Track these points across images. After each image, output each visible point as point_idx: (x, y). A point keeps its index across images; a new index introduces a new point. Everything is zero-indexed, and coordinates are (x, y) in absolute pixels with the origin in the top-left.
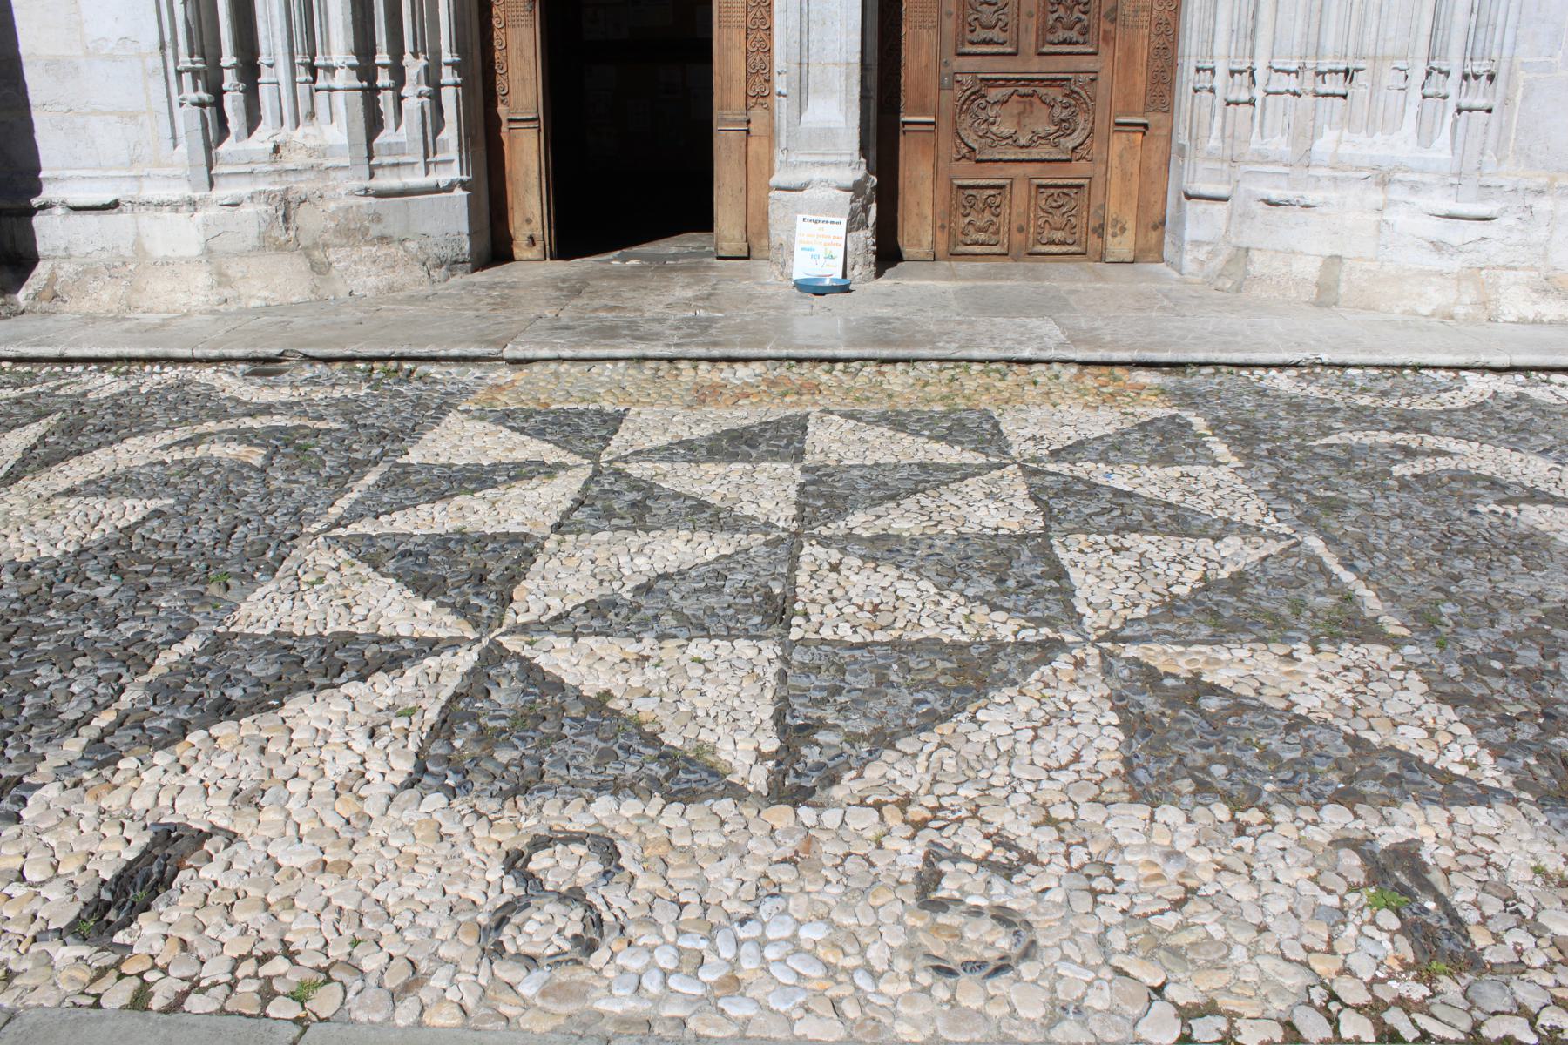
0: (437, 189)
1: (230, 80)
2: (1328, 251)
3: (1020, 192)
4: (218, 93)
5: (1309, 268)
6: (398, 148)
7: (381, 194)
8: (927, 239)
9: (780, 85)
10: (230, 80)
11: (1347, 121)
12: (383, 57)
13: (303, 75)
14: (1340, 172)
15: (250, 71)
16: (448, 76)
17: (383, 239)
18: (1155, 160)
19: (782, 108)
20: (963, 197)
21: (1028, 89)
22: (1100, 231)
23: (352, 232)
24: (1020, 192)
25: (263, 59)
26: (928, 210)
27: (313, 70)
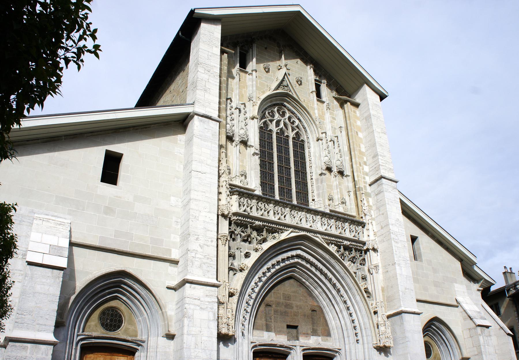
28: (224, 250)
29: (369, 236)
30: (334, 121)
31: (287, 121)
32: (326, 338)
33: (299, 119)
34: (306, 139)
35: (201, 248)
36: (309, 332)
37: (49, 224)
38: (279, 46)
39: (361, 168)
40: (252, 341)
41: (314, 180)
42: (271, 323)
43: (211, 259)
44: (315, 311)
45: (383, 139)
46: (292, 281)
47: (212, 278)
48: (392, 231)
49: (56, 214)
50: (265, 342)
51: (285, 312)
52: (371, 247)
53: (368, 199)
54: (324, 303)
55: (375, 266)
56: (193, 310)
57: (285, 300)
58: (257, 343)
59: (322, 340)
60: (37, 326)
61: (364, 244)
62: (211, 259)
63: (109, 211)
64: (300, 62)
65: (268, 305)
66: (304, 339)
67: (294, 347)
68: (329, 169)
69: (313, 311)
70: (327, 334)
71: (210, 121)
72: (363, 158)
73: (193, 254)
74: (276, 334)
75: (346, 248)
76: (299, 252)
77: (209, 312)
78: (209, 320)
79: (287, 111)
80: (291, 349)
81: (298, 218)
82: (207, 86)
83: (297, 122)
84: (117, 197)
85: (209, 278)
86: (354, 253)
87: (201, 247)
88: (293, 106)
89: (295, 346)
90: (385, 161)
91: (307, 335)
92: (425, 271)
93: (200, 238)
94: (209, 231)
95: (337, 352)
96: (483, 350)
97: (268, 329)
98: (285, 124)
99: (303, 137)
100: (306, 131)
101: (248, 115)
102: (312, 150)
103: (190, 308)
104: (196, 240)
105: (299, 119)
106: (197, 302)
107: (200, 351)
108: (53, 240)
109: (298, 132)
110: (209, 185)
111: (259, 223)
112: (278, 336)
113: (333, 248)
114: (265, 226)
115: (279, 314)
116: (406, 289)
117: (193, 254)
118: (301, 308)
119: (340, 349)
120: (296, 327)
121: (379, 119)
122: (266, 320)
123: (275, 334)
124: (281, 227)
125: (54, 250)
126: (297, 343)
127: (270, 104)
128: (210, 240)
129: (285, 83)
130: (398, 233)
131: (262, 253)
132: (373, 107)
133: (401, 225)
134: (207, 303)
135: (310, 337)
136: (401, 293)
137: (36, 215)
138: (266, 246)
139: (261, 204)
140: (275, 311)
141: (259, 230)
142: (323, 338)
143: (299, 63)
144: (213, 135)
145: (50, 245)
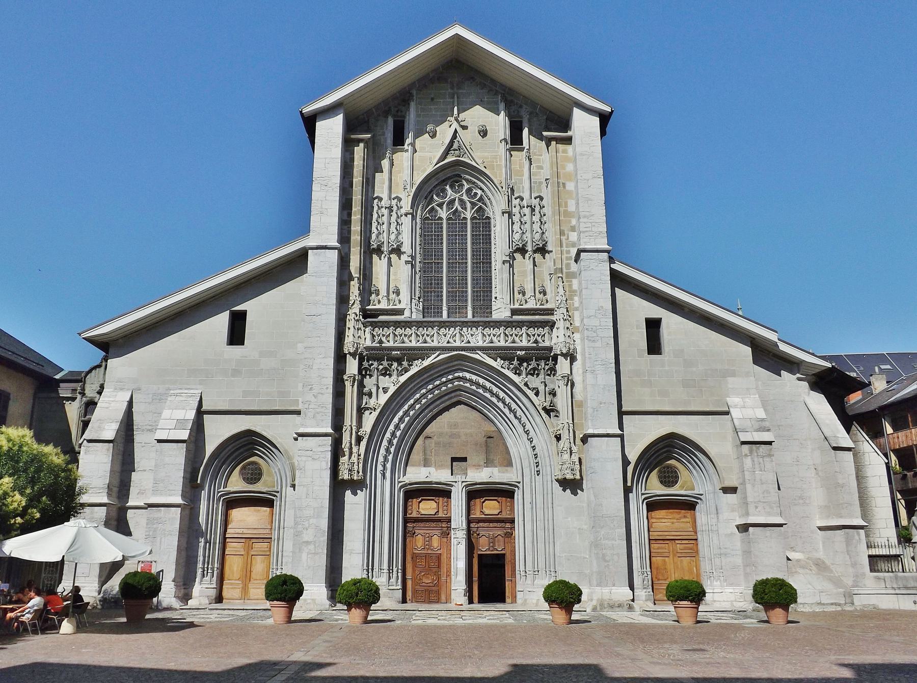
0: (398, 589)
1: (370, 570)
2: (537, 598)
4: (368, 573)
5: (535, 601)
6: (392, 582)
9: (452, 573)
10: (370, 570)
12: (391, 568)
13: (380, 570)
15: (372, 569)
16: (400, 571)
18: (513, 586)
19: (453, 577)
25: (374, 568)
27: (381, 569)
29: (558, 337)
30: (540, 172)
31: (465, 197)
33: (481, 189)
34: (491, 215)
35: (315, 398)
36: (482, 463)
38: (452, 88)
39: (563, 238)
41: (497, 270)
42: (431, 457)
43: (325, 407)
44: (492, 437)
45: (593, 188)
47: (327, 427)
48: (588, 328)
49: (188, 387)
50: (411, 480)
51: (449, 443)
52: (559, 353)
53: (571, 281)
55: (562, 377)
56: (305, 461)
58: (407, 482)
61: (550, 349)
62: (325, 407)
63: (236, 372)
64: (487, 98)
65: (427, 437)
66: (474, 472)
68: (522, 250)
69: (490, 437)
70: (508, 463)
72: (570, 222)
73: (306, 406)
74: (436, 470)
75: (521, 360)
77: (322, 461)
78: (321, 469)
79: (465, 183)
80: (452, 486)
82: (323, 207)
83: (479, 192)
87: (315, 396)
89: (456, 482)
91: (478, 466)
92: (667, 368)
93: (314, 388)
94: (324, 377)
96: (747, 477)
98: (462, 202)
99: (489, 212)
100: (491, 204)
101: (403, 211)
102: (498, 228)
104: (310, 390)
105: (481, 189)
108: (180, 414)
110: (325, 328)
111: (396, 352)
112: (439, 471)
113: (497, 364)
114: (405, 354)
115: (442, 445)
116: (601, 404)
117: (306, 406)
118: (472, 436)
119: (519, 483)
120: (464, 459)
122: (425, 454)
123: (436, 469)
125: (180, 424)
126: (459, 478)
129: (455, 146)
130: (598, 328)
131: (398, 386)
134: (320, 453)
136: (590, 411)
137: (172, 392)
138: (403, 379)
140: (435, 444)
141: (399, 360)
142: (500, 468)
143: (486, 100)
144: (330, 267)
145: (177, 420)
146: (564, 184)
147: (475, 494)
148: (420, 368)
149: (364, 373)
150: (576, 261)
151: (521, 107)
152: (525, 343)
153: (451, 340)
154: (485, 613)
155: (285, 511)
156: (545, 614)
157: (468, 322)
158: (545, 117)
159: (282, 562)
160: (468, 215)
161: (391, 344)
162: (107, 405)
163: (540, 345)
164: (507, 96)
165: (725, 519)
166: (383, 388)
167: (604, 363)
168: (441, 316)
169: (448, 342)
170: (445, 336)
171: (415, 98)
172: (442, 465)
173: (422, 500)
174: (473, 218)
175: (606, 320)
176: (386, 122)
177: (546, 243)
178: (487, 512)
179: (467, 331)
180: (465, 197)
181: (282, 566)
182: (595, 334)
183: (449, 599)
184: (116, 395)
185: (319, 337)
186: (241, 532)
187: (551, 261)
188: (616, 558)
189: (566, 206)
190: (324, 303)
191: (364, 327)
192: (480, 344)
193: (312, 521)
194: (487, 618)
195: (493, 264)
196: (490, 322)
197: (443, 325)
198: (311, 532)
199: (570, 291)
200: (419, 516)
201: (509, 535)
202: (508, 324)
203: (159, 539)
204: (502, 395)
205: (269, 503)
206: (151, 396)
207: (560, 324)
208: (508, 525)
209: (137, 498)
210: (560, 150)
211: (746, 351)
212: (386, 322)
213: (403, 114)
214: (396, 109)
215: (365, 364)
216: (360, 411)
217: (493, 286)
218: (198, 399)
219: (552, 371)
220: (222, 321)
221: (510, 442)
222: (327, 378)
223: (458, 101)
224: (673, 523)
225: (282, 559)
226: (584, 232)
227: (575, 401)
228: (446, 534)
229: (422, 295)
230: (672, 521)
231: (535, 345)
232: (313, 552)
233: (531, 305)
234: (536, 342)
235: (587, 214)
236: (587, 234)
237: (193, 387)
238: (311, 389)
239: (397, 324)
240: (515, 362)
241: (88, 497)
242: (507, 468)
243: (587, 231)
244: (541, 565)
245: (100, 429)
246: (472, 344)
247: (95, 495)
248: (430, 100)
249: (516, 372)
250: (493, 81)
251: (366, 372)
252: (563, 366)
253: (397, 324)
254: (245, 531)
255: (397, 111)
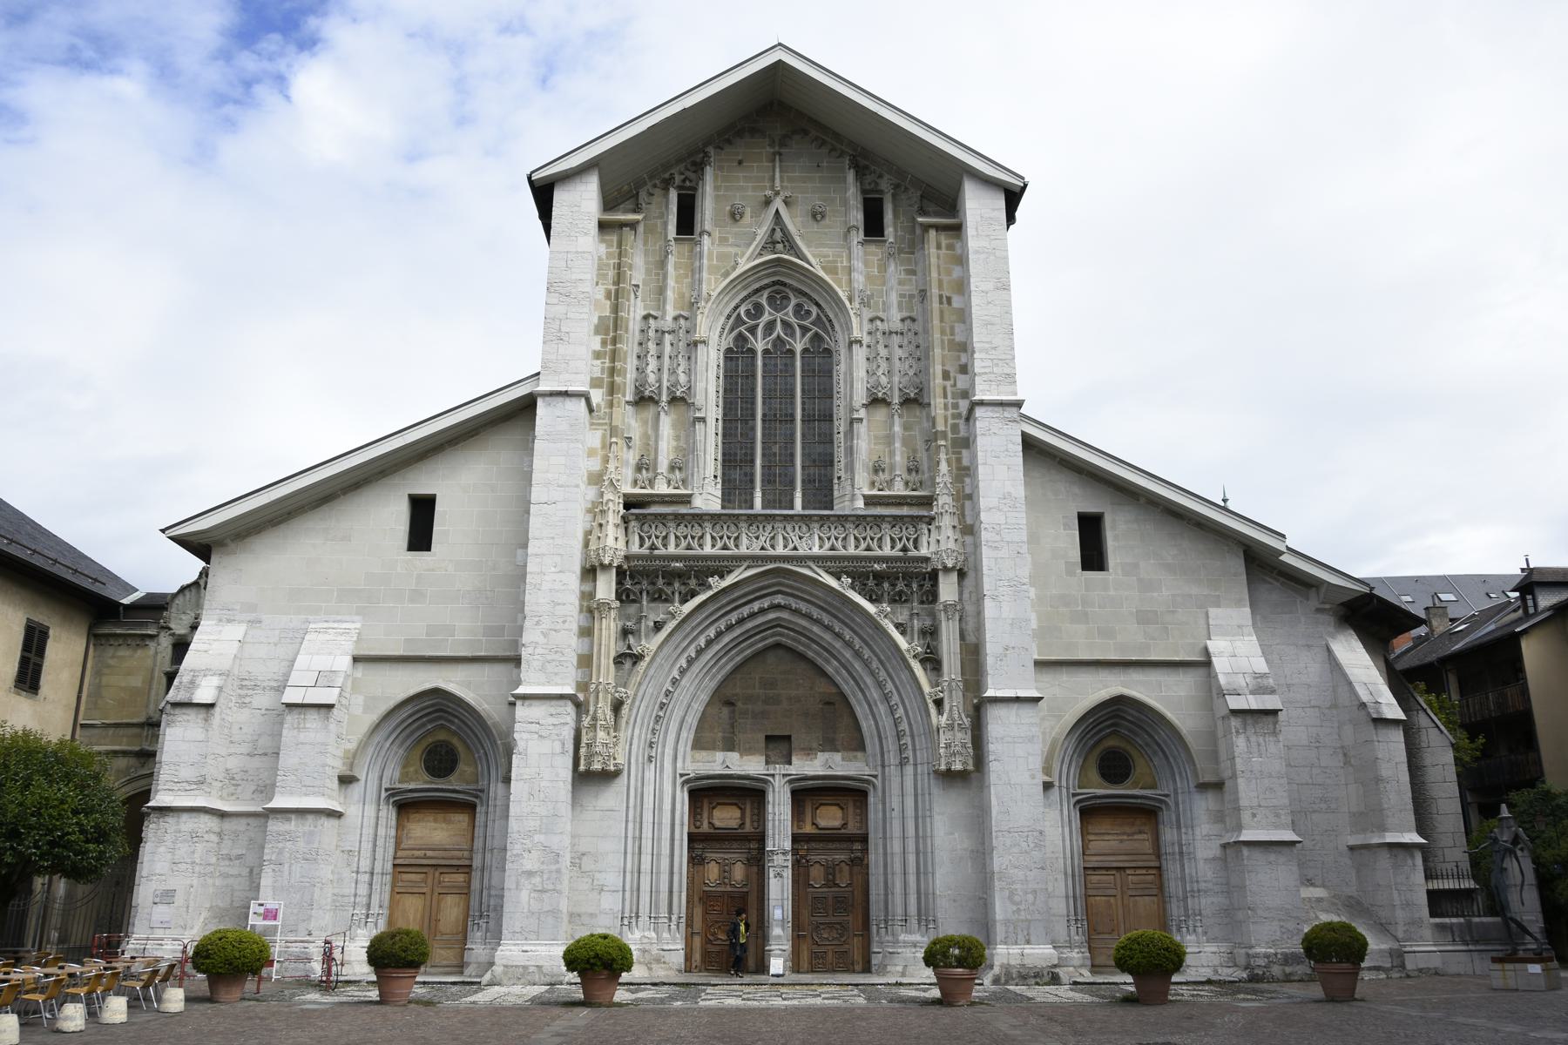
3: (830, 954)
7: (663, 950)
8: (806, 966)
11: (906, 932)
14: (906, 944)
17: (664, 963)
20: (814, 955)
21: (830, 926)
22: (853, 964)
23: (658, 961)
24: (830, 954)
26: (806, 958)
28: (609, 628)
31: (793, 320)
32: (851, 754)
36: (815, 745)
37: (327, 637)
39: (948, 384)
40: (682, 772)
46: (781, 652)
49: (339, 618)
53: (960, 453)
54: (848, 688)
57: (765, 689)
59: (843, 759)
60: (304, 789)
61: (926, 560)
63: (417, 595)
67: (770, 779)
69: (828, 703)
71: (568, 399)
72: (959, 358)
73: (530, 650)
74: (741, 755)
76: (779, 599)
77: (553, 741)
79: (791, 296)
81: (763, 539)
82: (563, 329)
83: (814, 310)
84: (428, 570)
85: (557, 684)
86: (900, 586)
87: (545, 635)
88: (799, 281)
89: (773, 775)
90: (992, 360)
91: (809, 751)
92: (1112, 592)
94: (559, 604)
95: (868, 782)
97: (729, 746)
98: (786, 324)
103: (521, 739)
106: (534, 727)
107: (537, 804)
108: (323, 662)
109: (816, 334)
111: (677, 565)
114: (691, 566)
119: (875, 777)
120: (788, 738)
121: (992, 258)
124: (726, 563)
126: (780, 769)
127: (745, 293)
128: (560, 620)
130: (1003, 527)
132: (980, 228)
133: (1017, 505)
135: (816, 754)
137: (312, 626)
139: (686, 526)
143: (825, 164)
146: (949, 300)
147: (806, 795)
148: (716, 590)
149: (624, 598)
150: (968, 419)
151: (880, 176)
152: (887, 551)
153: (768, 545)
154: (820, 989)
155: (494, 821)
156: (917, 989)
157: (796, 515)
158: (919, 193)
159: (489, 906)
160: (799, 347)
161: (672, 549)
162: (205, 647)
163: (910, 554)
164: (858, 158)
165: (1204, 833)
166: (655, 623)
167: (1012, 584)
168: (752, 507)
169: (763, 548)
170: (757, 538)
171: (712, 159)
172: (750, 748)
173: (719, 804)
174: (805, 351)
175: (1016, 515)
176: (666, 195)
177: (921, 390)
178: (823, 823)
179: (794, 530)
180: (793, 320)
181: (488, 911)
182: (998, 538)
183: (763, 968)
184: (221, 631)
185: (553, 538)
186: (422, 855)
187: (928, 421)
188: (1030, 897)
189: (952, 334)
190: (560, 483)
191: (625, 522)
192: (816, 550)
193: (537, 838)
194: (823, 996)
195: (836, 423)
196: (828, 517)
197: (752, 519)
198: (535, 854)
199: (959, 469)
200: (712, 831)
201: (860, 864)
202: (859, 520)
203: (286, 866)
204: (848, 635)
205: (470, 808)
206: (277, 632)
207: (947, 522)
208: (857, 846)
209: (253, 799)
210: (943, 245)
211: (1237, 565)
212: (660, 515)
213: (693, 184)
214: (683, 177)
215: (628, 584)
216: (619, 660)
217: (836, 460)
218: (355, 639)
219: (932, 596)
220: (393, 515)
221: (861, 711)
222: (564, 604)
223: (781, 167)
224: (1121, 841)
225: (489, 901)
226: (980, 374)
227: (966, 645)
228: (758, 861)
229: (719, 473)
230: (1120, 837)
231: (901, 554)
232: (540, 888)
233: (899, 489)
234: (904, 549)
235: (987, 346)
236: (985, 377)
237: (347, 618)
238: (538, 623)
239: (679, 519)
240: (871, 583)
241: (172, 798)
242: (855, 753)
243: (986, 373)
244: (913, 910)
245: (193, 684)
246: (801, 552)
247: (183, 793)
248: (736, 164)
249: (871, 597)
250: (837, 136)
251: (628, 596)
252: (948, 590)
253: (679, 519)
254: (429, 853)
255: (684, 181)
